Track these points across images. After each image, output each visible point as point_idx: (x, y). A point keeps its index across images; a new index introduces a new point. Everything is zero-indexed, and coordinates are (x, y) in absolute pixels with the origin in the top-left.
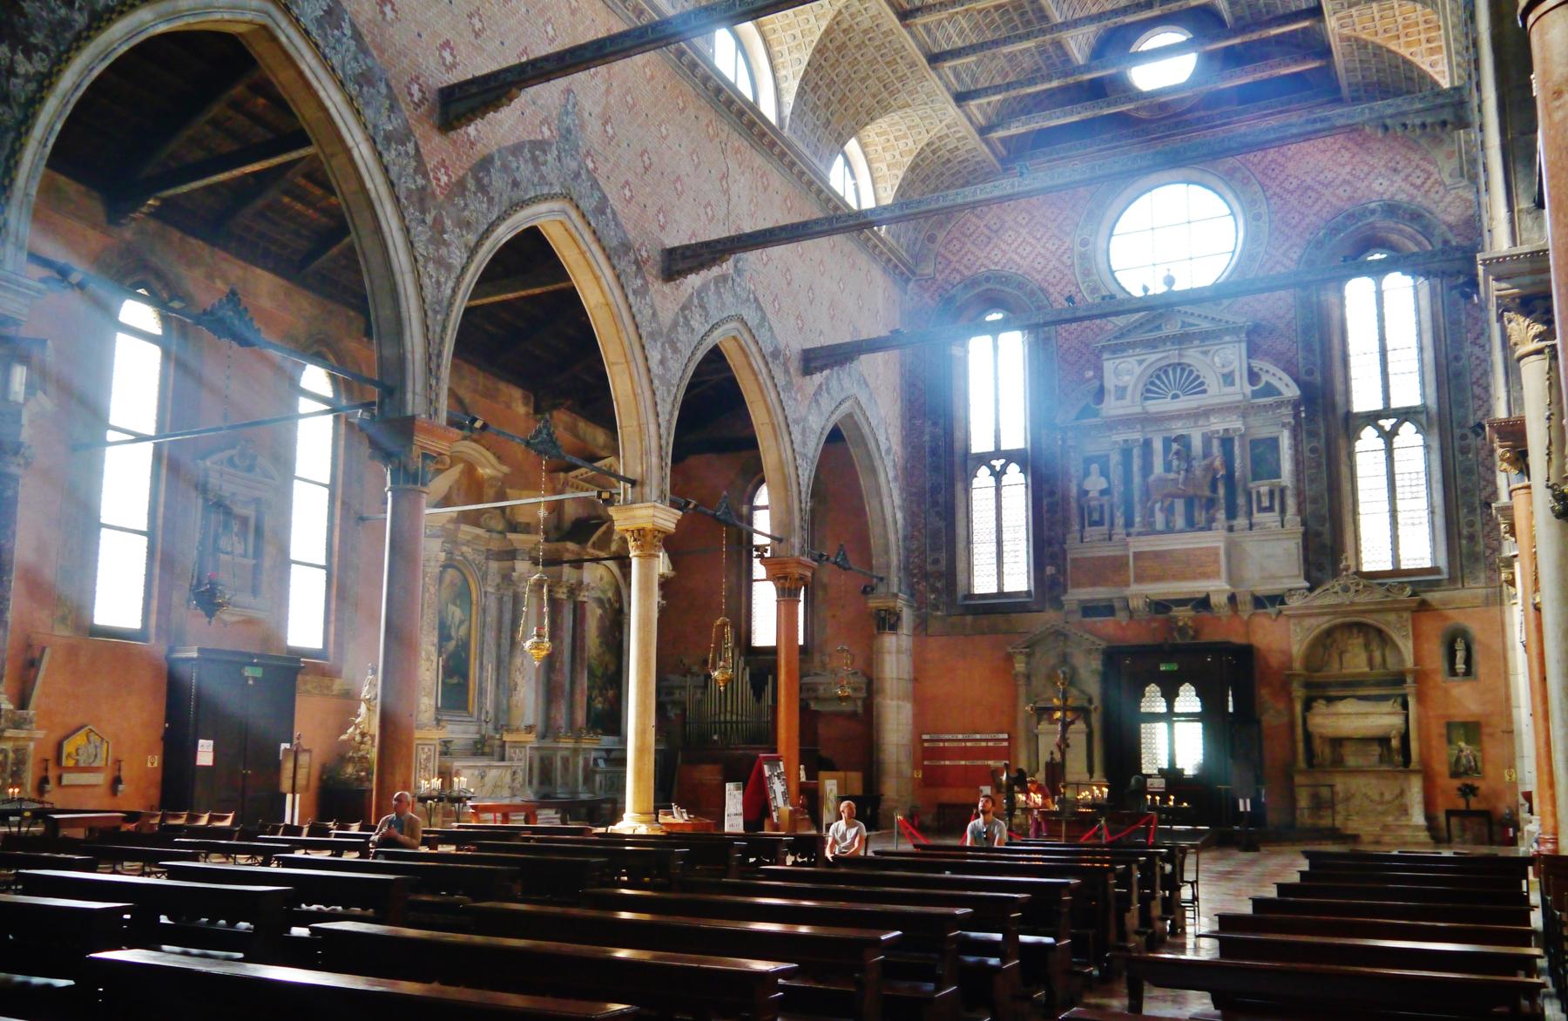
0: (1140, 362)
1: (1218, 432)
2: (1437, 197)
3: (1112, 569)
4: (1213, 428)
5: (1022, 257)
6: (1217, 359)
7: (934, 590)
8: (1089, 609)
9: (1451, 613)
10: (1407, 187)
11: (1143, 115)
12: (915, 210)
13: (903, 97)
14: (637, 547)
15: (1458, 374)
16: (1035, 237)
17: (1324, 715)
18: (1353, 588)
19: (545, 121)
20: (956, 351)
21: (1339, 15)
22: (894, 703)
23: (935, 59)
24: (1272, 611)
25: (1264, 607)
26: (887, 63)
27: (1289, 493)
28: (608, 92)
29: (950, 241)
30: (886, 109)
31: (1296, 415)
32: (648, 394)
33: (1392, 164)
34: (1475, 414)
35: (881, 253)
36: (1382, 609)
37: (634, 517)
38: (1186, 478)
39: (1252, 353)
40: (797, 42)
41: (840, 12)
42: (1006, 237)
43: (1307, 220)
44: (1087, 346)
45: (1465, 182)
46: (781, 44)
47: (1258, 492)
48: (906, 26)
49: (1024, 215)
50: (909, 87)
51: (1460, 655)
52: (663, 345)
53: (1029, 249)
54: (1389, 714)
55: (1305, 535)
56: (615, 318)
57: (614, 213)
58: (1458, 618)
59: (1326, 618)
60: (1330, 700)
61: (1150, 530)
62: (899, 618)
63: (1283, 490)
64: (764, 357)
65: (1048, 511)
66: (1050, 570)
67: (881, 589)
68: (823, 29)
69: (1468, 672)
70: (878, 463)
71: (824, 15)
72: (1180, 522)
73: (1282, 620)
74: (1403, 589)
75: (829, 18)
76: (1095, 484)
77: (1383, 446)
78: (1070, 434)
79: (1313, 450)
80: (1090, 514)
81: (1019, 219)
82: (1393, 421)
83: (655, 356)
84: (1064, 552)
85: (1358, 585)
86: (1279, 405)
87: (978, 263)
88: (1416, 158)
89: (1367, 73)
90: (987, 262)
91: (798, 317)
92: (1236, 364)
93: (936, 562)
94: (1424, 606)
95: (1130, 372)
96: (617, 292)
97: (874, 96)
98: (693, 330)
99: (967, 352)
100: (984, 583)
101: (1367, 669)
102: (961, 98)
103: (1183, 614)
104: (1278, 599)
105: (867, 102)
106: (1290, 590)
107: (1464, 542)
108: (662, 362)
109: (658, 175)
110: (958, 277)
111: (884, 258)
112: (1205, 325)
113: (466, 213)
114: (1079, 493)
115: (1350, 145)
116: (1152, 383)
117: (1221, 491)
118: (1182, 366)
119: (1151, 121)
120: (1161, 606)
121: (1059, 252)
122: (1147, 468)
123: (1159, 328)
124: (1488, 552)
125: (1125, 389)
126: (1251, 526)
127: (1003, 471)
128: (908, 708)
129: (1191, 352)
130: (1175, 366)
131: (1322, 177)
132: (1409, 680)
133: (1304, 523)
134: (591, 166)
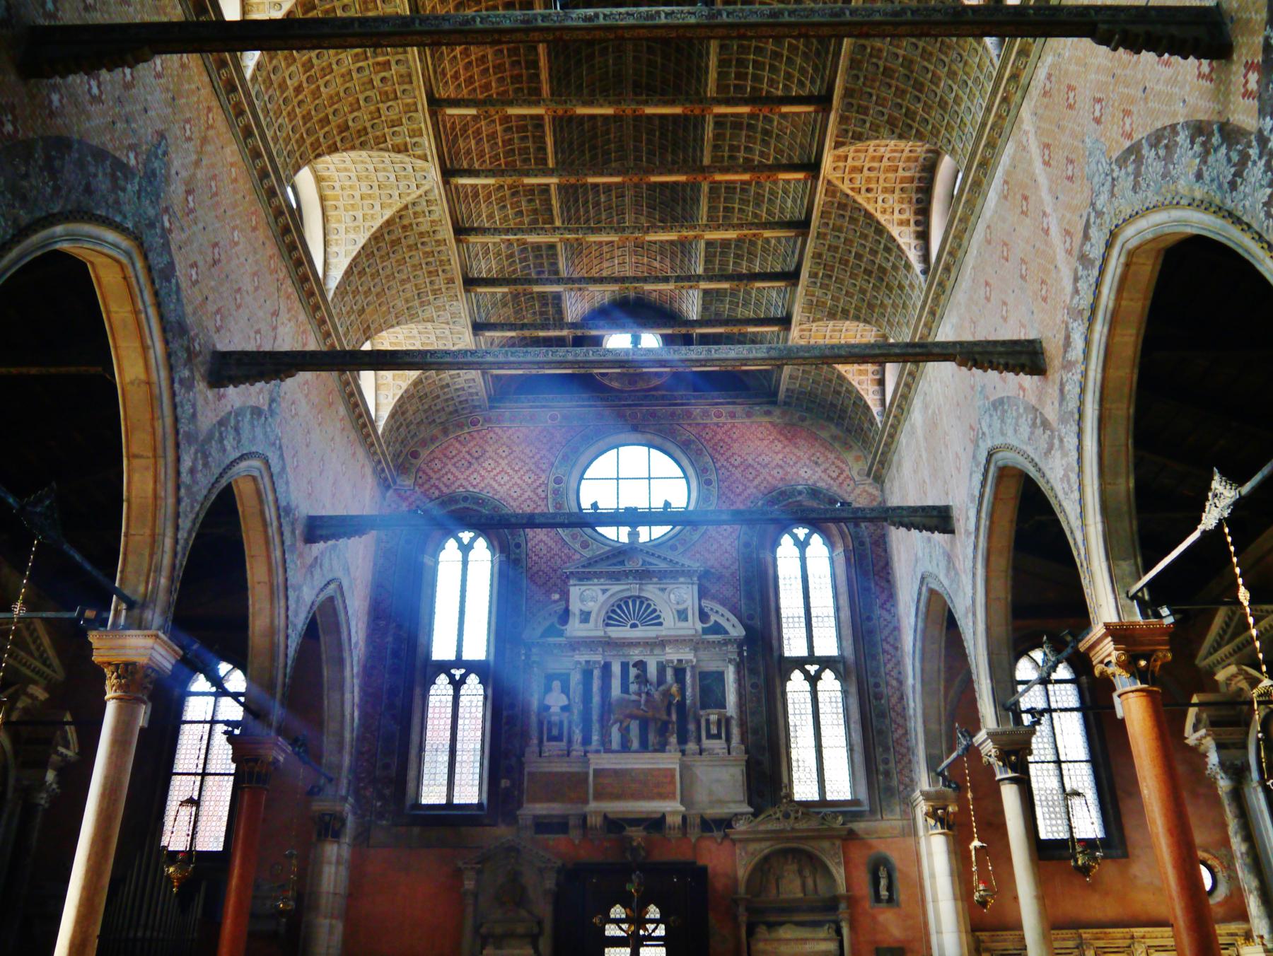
0: (604, 591)
1: (672, 661)
2: (849, 489)
3: (573, 785)
4: (668, 657)
5: (500, 485)
6: (672, 596)
7: (381, 796)
8: (543, 825)
9: (874, 842)
10: (824, 476)
11: (615, 385)
12: (521, 359)
13: (430, 311)
14: (120, 687)
15: (871, 632)
16: (513, 469)
17: (765, 940)
18: (793, 815)
19: (132, 147)
20: (427, 560)
21: (804, 327)
22: (326, 922)
23: (470, 282)
24: (718, 834)
25: (711, 830)
26: (430, 272)
27: (734, 723)
28: (197, 163)
29: (431, 461)
30: (413, 317)
31: (740, 654)
32: (171, 500)
33: (814, 458)
34: (885, 665)
35: (375, 453)
36: (819, 836)
37: (123, 647)
38: (647, 701)
39: (703, 593)
40: (356, 224)
41: (406, 207)
42: (486, 465)
43: (749, 491)
44: (555, 571)
45: (870, 481)
46: (339, 221)
47: (708, 721)
48: (458, 241)
49: (504, 448)
50: (439, 303)
51: (883, 882)
52: (196, 453)
53: (506, 478)
54: (825, 940)
55: (748, 762)
56: (153, 400)
57: (177, 284)
58: (882, 848)
59: (768, 844)
60: (772, 926)
61: (606, 747)
62: (343, 822)
63: (728, 720)
64: (278, 508)
65: (507, 723)
66: (504, 783)
67: (330, 790)
68: (386, 217)
69: (890, 900)
70: (346, 655)
71: (390, 205)
72: (635, 744)
73: (727, 843)
74: (836, 818)
75: (395, 209)
76: (556, 700)
77: (808, 688)
78: (534, 650)
79: (754, 686)
80: (550, 730)
81: (500, 451)
82: (816, 667)
83: (187, 463)
84: (521, 765)
85: (797, 812)
86: (726, 643)
87: (457, 484)
88: (832, 456)
89: (804, 383)
90: (465, 484)
91: (309, 482)
92: (689, 603)
93: (387, 766)
94: (852, 836)
95: (594, 599)
96: (163, 373)
97: (407, 301)
98: (225, 450)
99: (437, 563)
100: (432, 794)
101: (801, 895)
102: (478, 327)
103: (637, 835)
104: (725, 824)
105: (399, 304)
106: (736, 815)
107: (881, 777)
108: (192, 471)
109: (223, 276)
110: (437, 493)
111: (376, 458)
112: (663, 566)
113: (25, 183)
114: (539, 709)
115: (782, 438)
116: (613, 611)
117: (674, 717)
118: (642, 600)
119: (621, 391)
120: (615, 825)
121: (535, 485)
122: (606, 687)
123: (622, 563)
124: (901, 788)
125: (589, 613)
126: (701, 752)
127: (463, 680)
128: (339, 926)
129: (650, 587)
130: (634, 598)
131: (760, 459)
132: (843, 906)
133: (747, 752)
134: (167, 224)
